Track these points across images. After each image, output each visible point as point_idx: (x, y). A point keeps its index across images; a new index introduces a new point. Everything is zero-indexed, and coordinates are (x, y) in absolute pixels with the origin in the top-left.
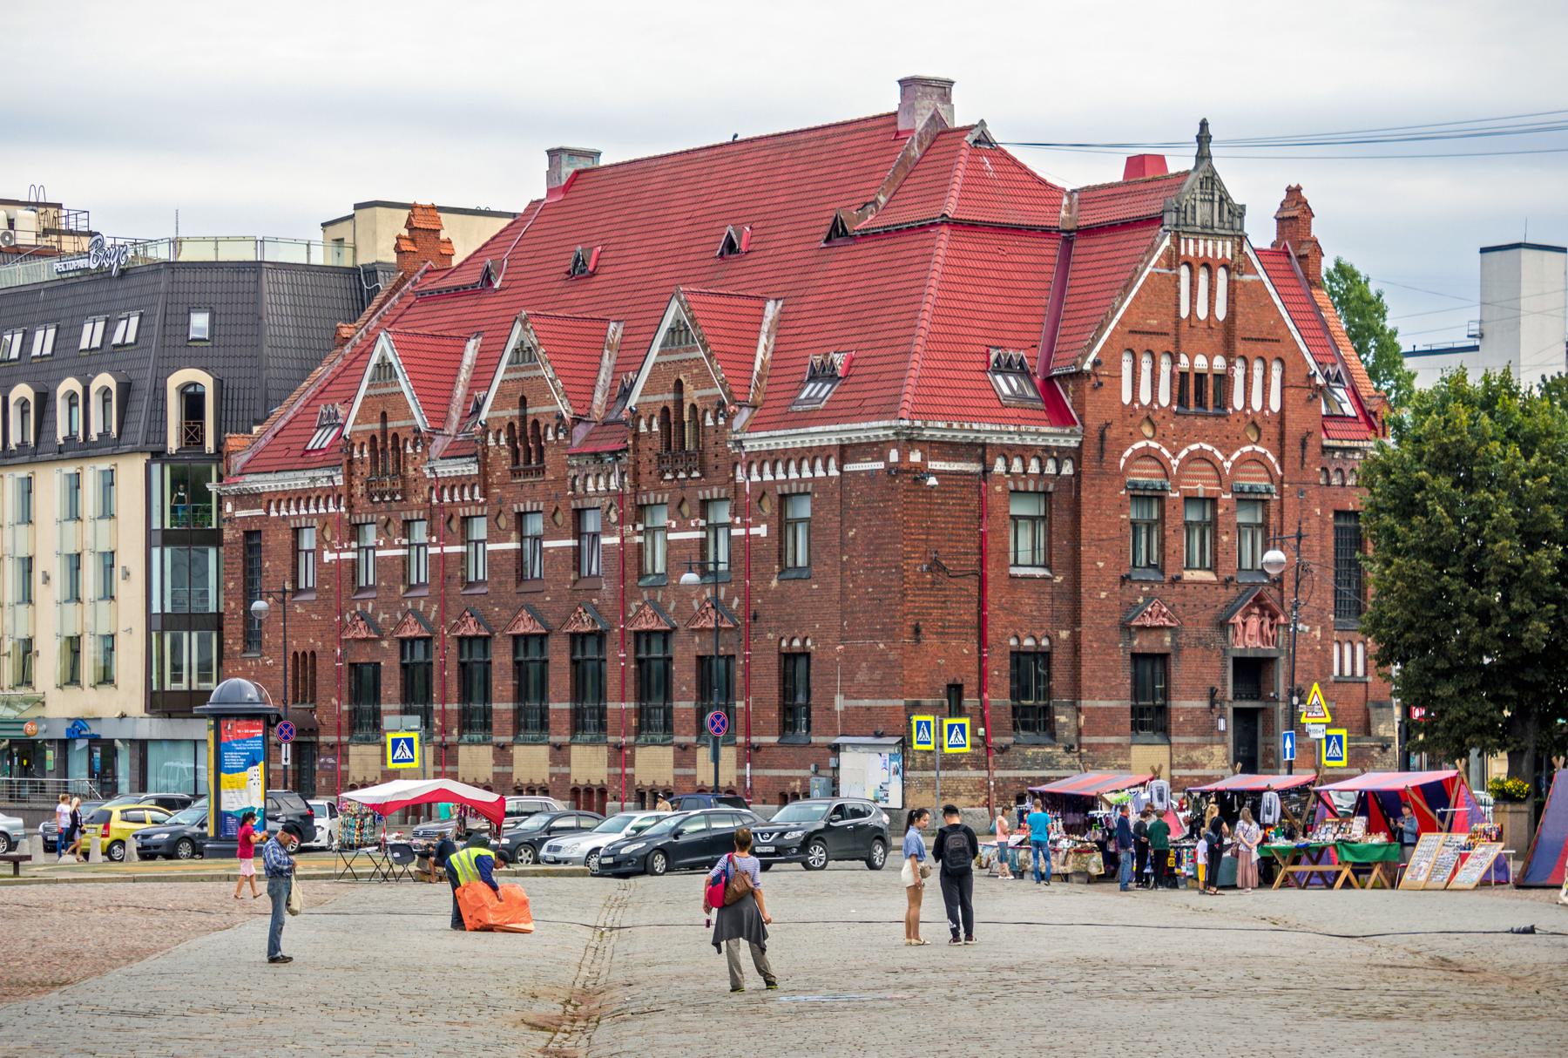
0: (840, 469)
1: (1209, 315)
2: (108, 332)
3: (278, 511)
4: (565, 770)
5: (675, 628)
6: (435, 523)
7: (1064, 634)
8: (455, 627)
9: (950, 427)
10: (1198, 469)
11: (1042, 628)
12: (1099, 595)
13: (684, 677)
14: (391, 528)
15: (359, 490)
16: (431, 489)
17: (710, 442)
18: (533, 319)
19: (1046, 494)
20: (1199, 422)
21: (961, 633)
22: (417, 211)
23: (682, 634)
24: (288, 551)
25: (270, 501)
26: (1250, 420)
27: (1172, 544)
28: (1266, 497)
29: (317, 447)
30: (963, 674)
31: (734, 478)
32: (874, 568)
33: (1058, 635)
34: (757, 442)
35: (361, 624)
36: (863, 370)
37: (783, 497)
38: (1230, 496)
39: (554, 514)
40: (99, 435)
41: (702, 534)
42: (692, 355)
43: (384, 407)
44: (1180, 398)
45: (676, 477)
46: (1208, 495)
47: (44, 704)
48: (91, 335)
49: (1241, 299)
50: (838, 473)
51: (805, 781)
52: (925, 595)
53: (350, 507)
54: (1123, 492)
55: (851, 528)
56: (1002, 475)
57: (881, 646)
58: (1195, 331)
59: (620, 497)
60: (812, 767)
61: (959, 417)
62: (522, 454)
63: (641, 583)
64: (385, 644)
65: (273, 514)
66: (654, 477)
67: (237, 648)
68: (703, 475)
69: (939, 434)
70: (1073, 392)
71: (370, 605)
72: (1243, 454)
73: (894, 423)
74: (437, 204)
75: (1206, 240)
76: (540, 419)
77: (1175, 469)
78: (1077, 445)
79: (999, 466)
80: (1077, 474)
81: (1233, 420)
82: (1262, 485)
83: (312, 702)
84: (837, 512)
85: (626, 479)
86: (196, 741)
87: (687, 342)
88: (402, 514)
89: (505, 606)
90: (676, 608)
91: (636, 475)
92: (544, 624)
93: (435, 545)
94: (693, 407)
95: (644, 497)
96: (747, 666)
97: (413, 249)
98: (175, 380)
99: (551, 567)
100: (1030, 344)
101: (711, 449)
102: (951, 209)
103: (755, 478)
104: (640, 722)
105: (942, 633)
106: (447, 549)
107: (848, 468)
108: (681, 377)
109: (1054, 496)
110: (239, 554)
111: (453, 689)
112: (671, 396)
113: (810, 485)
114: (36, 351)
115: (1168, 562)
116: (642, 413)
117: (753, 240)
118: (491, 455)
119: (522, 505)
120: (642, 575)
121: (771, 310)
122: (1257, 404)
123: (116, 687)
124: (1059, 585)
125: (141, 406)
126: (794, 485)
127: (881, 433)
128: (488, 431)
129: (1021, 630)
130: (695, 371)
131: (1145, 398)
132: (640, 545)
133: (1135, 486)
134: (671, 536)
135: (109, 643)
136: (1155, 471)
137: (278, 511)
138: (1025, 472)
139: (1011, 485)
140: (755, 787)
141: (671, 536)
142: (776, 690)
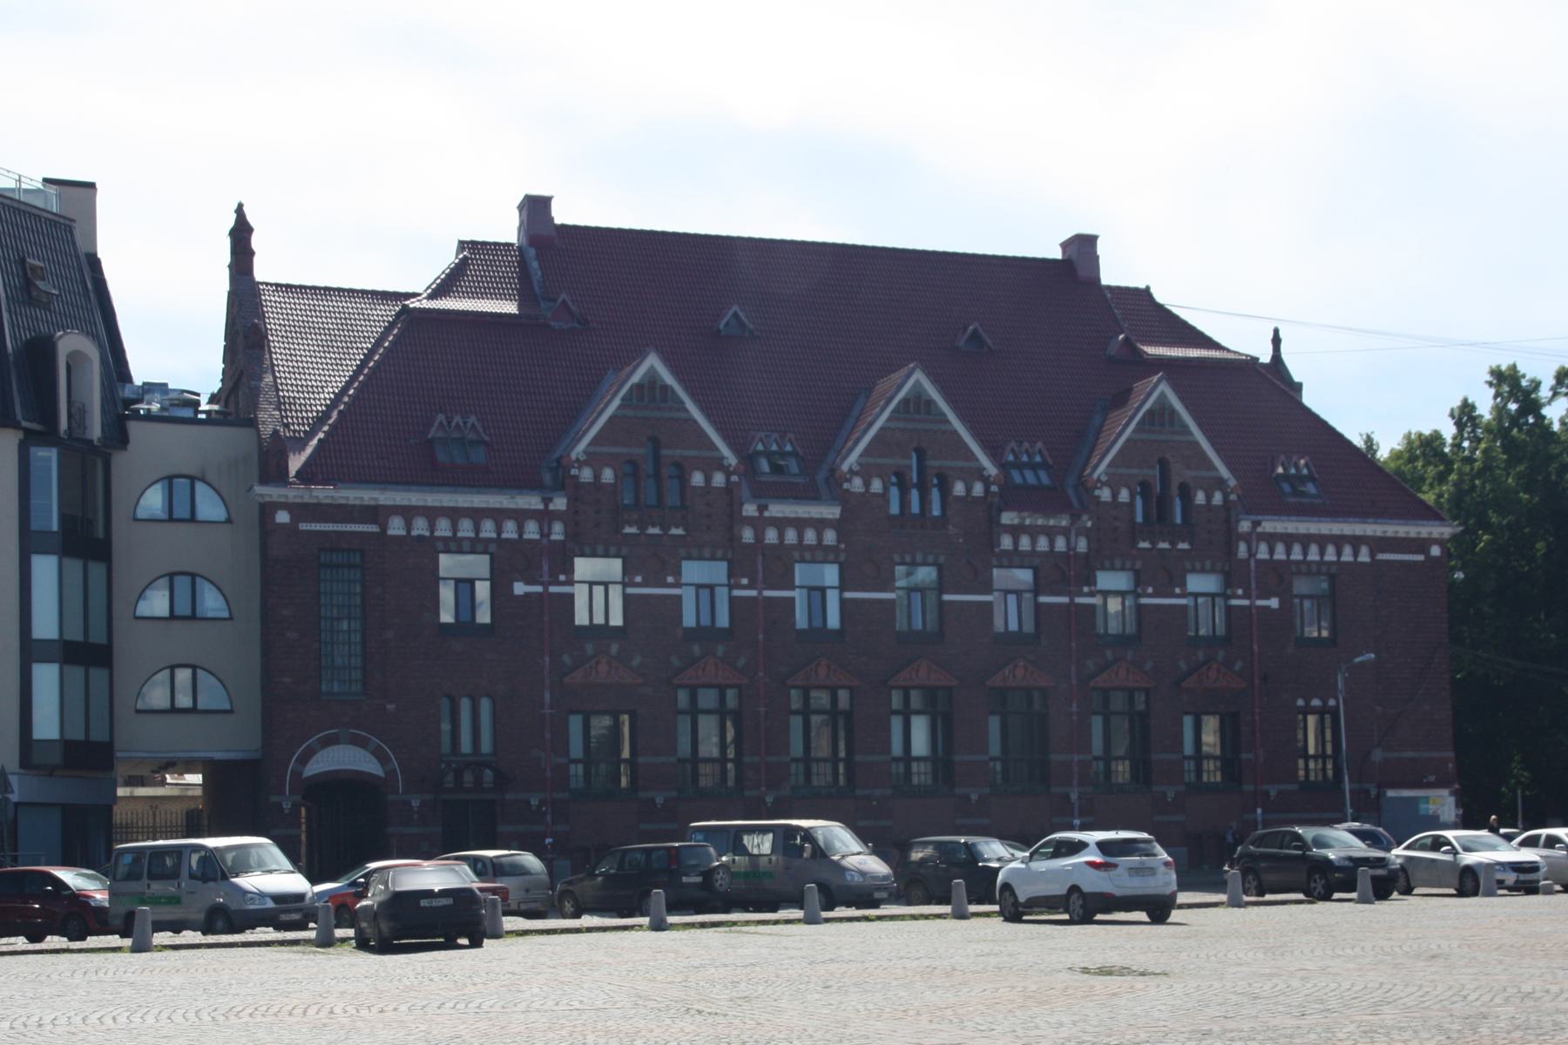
0: (1372, 555)
59: (1070, 556)
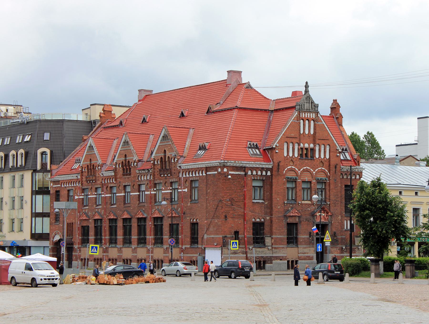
0: (206, 173)
1: (309, 133)
2: (23, 138)
3: (64, 185)
4: (136, 254)
5: (164, 216)
6: (103, 188)
7: (268, 218)
8: (108, 216)
9: (235, 163)
10: (306, 174)
11: (261, 216)
12: (278, 207)
13: (166, 229)
14: (92, 190)
15: (84, 179)
16: (102, 179)
17: (173, 166)
18: (129, 134)
19: (263, 180)
20: (306, 161)
21: (238, 218)
22: (106, 106)
23: (165, 218)
24: (66, 196)
25: (62, 183)
26: (321, 161)
27: (298, 194)
28: (325, 181)
29: (74, 168)
30: (239, 228)
31: (179, 176)
32: (214, 200)
33: (266, 218)
34: (184, 166)
35: (84, 215)
36: (213, 147)
37: (191, 181)
38: (315, 181)
39: (133, 186)
40: (20, 165)
41: (171, 191)
42: (168, 143)
43: (90, 158)
44: (301, 155)
45: (164, 176)
46: (309, 181)
47: (5, 237)
48: (19, 139)
49: (317, 129)
50: (205, 175)
51: (197, 257)
52: (228, 207)
53: (82, 184)
54: (285, 180)
55: (209, 189)
56: (250, 175)
57: (216, 221)
58: (305, 137)
59: (150, 181)
60: (198, 253)
61: (238, 160)
62: (125, 170)
63: (155, 204)
64: (90, 221)
65: (63, 186)
66: (159, 176)
67: (53, 222)
68: (171, 175)
69: (232, 164)
70: (271, 153)
71: (87, 210)
72: (318, 170)
73: (219, 161)
74: (111, 104)
75: (308, 113)
76: (130, 160)
77: (299, 174)
78: (271, 167)
79: (249, 173)
80: (272, 175)
81: (316, 161)
82: (324, 178)
83: (72, 236)
84: (205, 185)
85: (152, 176)
86: (44, 247)
87: (167, 140)
88: (95, 186)
89: (121, 210)
90: (164, 211)
91: (154, 175)
92: (130, 216)
93: (103, 194)
94: (169, 157)
95: (156, 181)
96: (182, 226)
97: (104, 116)
98: (40, 151)
99: (132, 200)
100: (260, 140)
101: (173, 169)
102: (239, 104)
103: (184, 176)
104: (155, 241)
105: (233, 218)
106: (106, 195)
107: (208, 173)
108: (166, 149)
109: (265, 181)
110: (54, 197)
111: (108, 233)
112: (162, 155)
113: (198, 178)
114: (5, 144)
115: (297, 198)
116: (156, 159)
117: (188, 113)
118: (117, 170)
119: (125, 183)
120: (155, 202)
121: (191, 131)
122: (322, 156)
123: (23, 232)
124: (267, 205)
125: (31, 157)
126: (194, 178)
127: (216, 164)
128: (117, 164)
129: (256, 217)
130: (169, 148)
131: (291, 155)
132: (155, 194)
133: (288, 178)
134: (163, 192)
135: (21, 221)
136: (294, 174)
137: (64, 185)
138: (257, 174)
139: (253, 178)
140: (184, 259)
141: (163, 192)
142: (189, 233)
